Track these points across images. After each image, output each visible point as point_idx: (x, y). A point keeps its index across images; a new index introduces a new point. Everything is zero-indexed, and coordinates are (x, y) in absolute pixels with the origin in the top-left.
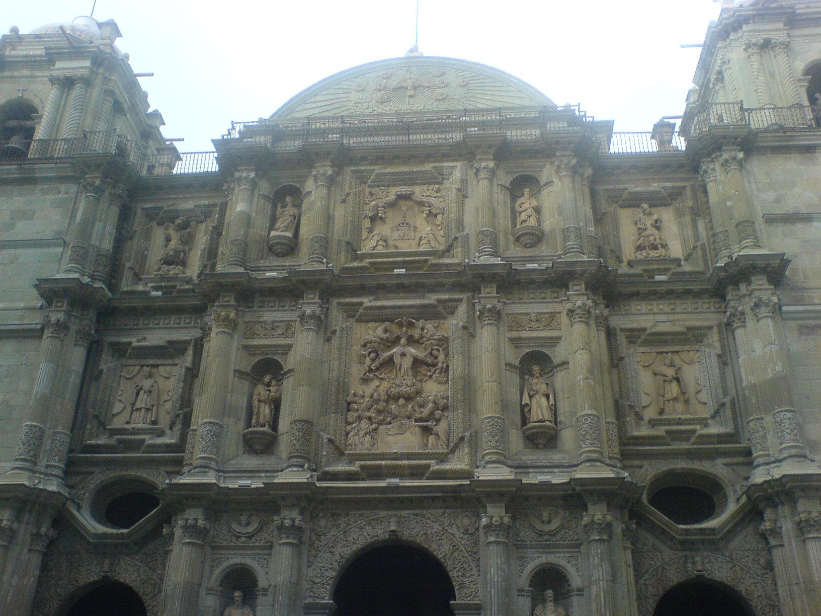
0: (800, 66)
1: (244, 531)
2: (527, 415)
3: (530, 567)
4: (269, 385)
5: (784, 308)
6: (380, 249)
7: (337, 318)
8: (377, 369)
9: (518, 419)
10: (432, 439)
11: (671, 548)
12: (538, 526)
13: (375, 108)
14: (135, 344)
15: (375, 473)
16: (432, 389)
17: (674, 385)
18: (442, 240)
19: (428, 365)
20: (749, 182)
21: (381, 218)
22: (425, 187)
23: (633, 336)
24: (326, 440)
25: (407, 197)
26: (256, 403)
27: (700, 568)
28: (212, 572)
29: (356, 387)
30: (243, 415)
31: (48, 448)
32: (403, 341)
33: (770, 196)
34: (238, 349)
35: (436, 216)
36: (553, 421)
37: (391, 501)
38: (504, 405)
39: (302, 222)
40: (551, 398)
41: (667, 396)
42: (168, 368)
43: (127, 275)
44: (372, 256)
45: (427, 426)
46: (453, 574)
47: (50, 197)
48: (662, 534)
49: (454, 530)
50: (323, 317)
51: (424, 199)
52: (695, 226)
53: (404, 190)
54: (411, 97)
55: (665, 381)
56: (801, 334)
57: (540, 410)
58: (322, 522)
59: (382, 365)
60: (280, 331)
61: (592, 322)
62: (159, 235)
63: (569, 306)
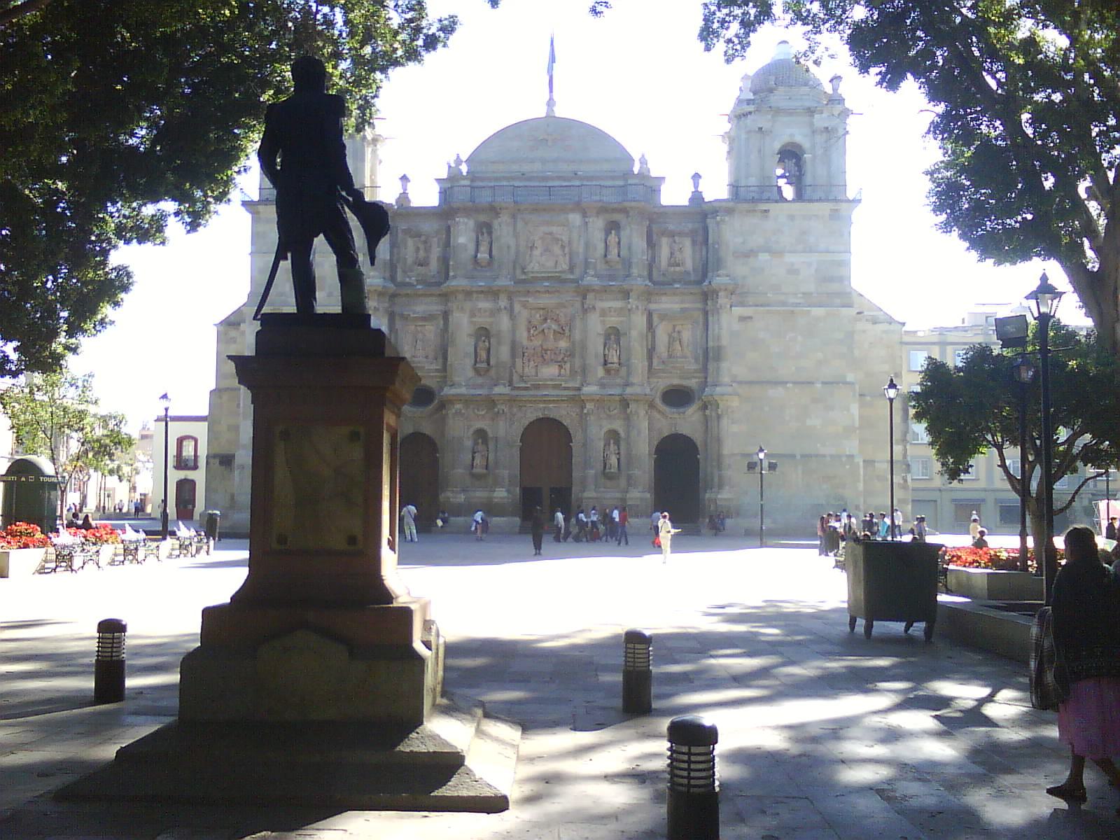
0: (777, 146)
3: (605, 430)
4: (484, 341)
6: (536, 268)
7: (517, 307)
8: (537, 335)
9: (602, 360)
14: (412, 316)
15: (537, 387)
16: (563, 344)
17: (678, 342)
18: (567, 261)
21: (536, 247)
22: (559, 228)
23: (664, 317)
25: (551, 234)
26: (478, 349)
28: (468, 429)
29: (525, 342)
32: (549, 321)
33: (740, 240)
38: (596, 356)
40: (618, 351)
44: (532, 272)
49: (572, 413)
51: (558, 236)
59: (539, 333)
60: (487, 313)
61: (640, 313)
62: (410, 243)
63: (629, 306)
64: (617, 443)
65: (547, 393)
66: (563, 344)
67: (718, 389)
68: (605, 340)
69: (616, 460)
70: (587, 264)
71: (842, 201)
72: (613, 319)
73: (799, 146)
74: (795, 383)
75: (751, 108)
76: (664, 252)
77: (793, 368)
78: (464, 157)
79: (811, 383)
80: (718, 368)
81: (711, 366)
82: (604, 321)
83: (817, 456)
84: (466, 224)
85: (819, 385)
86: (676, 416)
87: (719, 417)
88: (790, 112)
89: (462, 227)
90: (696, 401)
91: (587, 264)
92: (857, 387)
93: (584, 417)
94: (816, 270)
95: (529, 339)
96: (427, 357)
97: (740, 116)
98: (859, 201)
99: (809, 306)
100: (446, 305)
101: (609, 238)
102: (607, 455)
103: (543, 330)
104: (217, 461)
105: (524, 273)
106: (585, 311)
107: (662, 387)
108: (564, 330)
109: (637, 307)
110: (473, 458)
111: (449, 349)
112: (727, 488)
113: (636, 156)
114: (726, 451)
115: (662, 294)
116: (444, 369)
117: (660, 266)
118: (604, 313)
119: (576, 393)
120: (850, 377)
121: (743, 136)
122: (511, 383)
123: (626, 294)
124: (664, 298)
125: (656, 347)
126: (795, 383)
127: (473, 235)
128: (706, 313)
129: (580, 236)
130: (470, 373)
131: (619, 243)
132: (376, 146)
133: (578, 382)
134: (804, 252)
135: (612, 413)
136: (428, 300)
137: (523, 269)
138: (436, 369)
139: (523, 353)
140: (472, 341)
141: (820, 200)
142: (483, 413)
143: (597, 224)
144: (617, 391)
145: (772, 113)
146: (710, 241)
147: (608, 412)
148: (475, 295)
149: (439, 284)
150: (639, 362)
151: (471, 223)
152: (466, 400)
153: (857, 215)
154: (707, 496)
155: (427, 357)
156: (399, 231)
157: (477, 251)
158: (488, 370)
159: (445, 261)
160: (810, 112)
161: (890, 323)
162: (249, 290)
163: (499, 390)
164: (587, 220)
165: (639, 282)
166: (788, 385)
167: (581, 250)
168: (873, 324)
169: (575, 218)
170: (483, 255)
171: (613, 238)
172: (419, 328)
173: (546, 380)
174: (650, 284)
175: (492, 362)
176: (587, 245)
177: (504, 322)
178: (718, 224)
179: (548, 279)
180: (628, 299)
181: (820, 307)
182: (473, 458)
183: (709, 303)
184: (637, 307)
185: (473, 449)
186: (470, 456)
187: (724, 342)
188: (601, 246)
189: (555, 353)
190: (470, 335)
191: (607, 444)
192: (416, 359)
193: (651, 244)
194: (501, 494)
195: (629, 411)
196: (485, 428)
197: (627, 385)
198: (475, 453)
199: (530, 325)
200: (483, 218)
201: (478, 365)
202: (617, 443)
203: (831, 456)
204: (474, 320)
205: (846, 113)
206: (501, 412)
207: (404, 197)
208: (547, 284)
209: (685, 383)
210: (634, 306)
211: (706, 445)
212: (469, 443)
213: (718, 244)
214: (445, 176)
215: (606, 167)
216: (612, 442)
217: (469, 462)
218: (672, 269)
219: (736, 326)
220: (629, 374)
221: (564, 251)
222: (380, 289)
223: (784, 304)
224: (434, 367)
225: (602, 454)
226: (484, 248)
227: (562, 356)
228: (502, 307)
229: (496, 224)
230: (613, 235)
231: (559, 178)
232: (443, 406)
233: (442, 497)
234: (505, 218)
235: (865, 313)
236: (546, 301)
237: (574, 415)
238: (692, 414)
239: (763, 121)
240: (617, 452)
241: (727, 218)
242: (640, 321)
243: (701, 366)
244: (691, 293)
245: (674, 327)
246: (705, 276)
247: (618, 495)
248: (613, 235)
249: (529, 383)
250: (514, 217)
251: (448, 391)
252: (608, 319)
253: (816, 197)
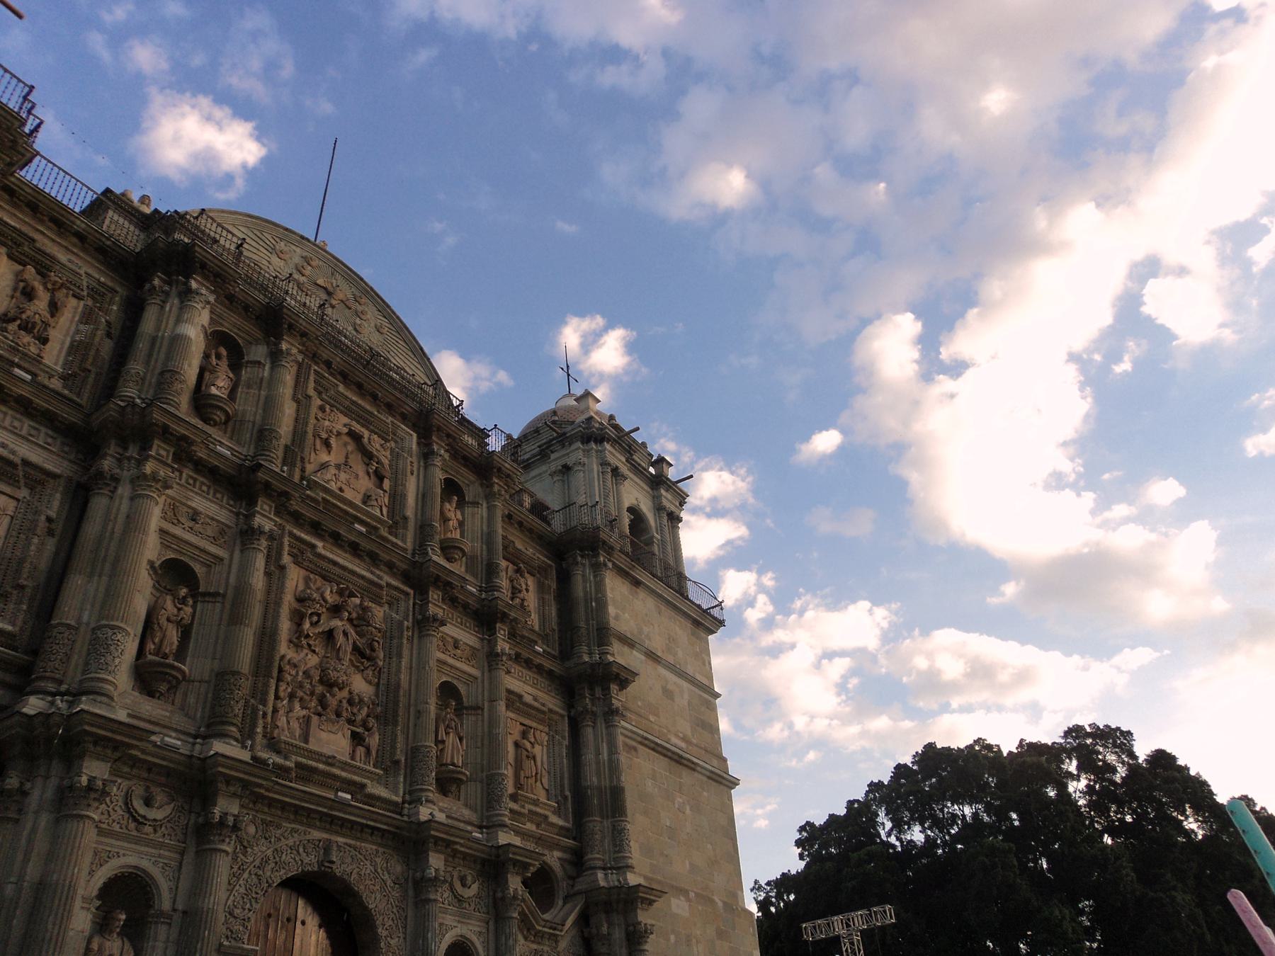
4: (183, 601)
10: (360, 751)
11: (526, 938)
28: (91, 873)
44: (326, 490)
108: (373, 650)
213: (597, 600)
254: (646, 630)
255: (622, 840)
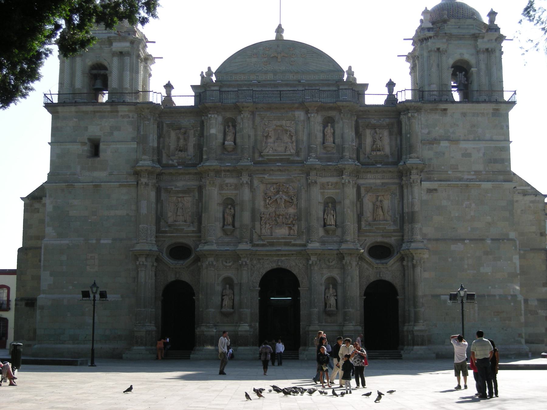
0: (451, 62)
1: (228, 264)
2: (325, 222)
3: (325, 277)
4: (230, 209)
5: (422, 182)
7: (256, 183)
9: (322, 223)
12: (328, 264)
13: (263, 68)
15: (272, 244)
16: (292, 210)
17: (380, 208)
18: (295, 148)
19: (290, 202)
20: (418, 124)
24: (254, 232)
25: (281, 126)
27: (381, 276)
28: (218, 278)
29: (262, 209)
30: (222, 220)
31: (150, 233)
32: (281, 193)
33: (425, 131)
34: (217, 195)
35: (292, 136)
36: (335, 224)
37: (278, 255)
39: (237, 136)
40: (335, 216)
41: (377, 213)
42: (188, 198)
43: (164, 155)
44: (268, 155)
45: (290, 227)
46: (299, 279)
47: (126, 120)
48: (370, 264)
50: (249, 183)
51: (287, 128)
52: (396, 140)
53: (279, 123)
54: (280, 62)
55: (377, 208)
56: (427, 192)
57: (331, 221)
58: (255, 262)
60: (233, 187)
62: (173, 134)
63: (343, 181)
64: (335, 286)
65: (280, 248)
66: (292, 210)
67: (413, 244)
68: (325, 207)
69: (335, 301)
70: (310, 149)
71: (501, 102)
72: (329, 191)
73: (467, 63)
74: (471, 240)
75: (431, 34)
76: (368, 141)
77: (469, 229)
78: (214, 70)
79: (482, 240)
80: (412, 229)
81: (407, 227)
82: (324, 192)
83: (489, 296)
84: (216, 119)
85: (489, 242)
86: (380, 266)
87: (414, 266)
88: (461, 37)
89: (213, 121)
90: (395, 254)
91: (310, 149)
92: (518, 242)
93: (309, 267)
94: (484, 155)
95: (266, 206)
96: (185, 221)
97: (422, 39)
98: (514, 103)
99: (480, 181)
100: (201, 181)
101: (326, 130)
102: (327, 297)
103: (276, 200)
104: (23, 303)
105: (261, 156)
106: (309, 185)
107: (368, 244)
108: (292, 200)
109: (349, 182)
110: (222, 300)
111: (203, 215)
112: (422, 321)
113: (345, 69)
114: (420, 293)
115: (368, 172)
116: (199, 230)
117: (366, 151)
118: (323, 186)
119: (303, 248)
120: (512, 235)
121: (425, 54)
122: (251, 241)
123: (340, 172)
124: (369, 176)
125: (364, 213)
126: (471, 240)
127: (222, 128)
128: (401, 187)
129: (304, 128)
130: (219, 233)
131: (334, 133)
132: (146, 63)
133: (304, 240)
134: (474, 140)
135: (331, 264)
136: (187, 177)
137: (260, 153)
138: (193, 231)
139: (261, 218)
140: (221, 209)
141: (485, 102)
142: (230, 264)
143: (317, 119)
144: (335, 247)
145: (447, 37)
146: (404, 132)
147: (328, 264)
148: (223, 173)
149: (195, 165)
150: (351, 225)
151: (220, 119)
152: (217, 255)
153: (513, 115)
154: (405, 328)
155: (185, 221)
156: (165, 125)
157: (224, 140)
158: (233, 231)
159: (199, 148)
160: (475, 37)
161: (536, 196)
162: (48, 171)
163: (243, 246)
164: (309, 115)
165: (350, 163)
166: (466, 241)
167: (305, 138)
168: (523, 195)
169: (300, 115)
170: (229, 143)
171: (329, 130)
172: (179, 199)
173: (278, 239)
174: (359, 164)
175: (237, 224)
176: (309, 135)
177: (246, 194)
178: (409, 119)
179: (281, 160)
180: (342, 175)
181: (487, 181)
182: (222, 300)
183: (404, 178)
184: (349, 182)
185: (222, 293)
186: (220, 298)
187: (417, 208)
188: (320, 136)
189: (286, 218)
190: (219, 204)
191: (327, 288)
192: (177, 223)
193: (359, 134)
194: (244, 328)
195: (344, 262)
196: (233, 277)
197: (342, 242)
198: (224, 296)
199: (266, 196)
200: (228, 115)
201: (225, 227)
202: (335, 286)
203: (500, 295)
204: (224, 192)
205: (502, 38)
206: (244, 263)
207: (168, 99)
208: (280, 164)
209: (386, 240)
210: (347, 181)
211: (404, 288)
212: (219, 288)
213: (410, 133)
214: (199, 83)
215: (322, 77)
216: (331, 286)
217: (219, 303)
218: (375, 153)
219: (425, 197)
220: (344, 233)
221: (291, 139)
222: (150, 168)
223: (460, 180)
224: (191, 229)
225: (323, 296)
226: (230, 137)
227: (291, 219)
228: (245, 182)
229: (239, 119)
230: (329, 127)
231: (287, 85)
232: (198, 259)
233: (198, 331)
234: (246, 114)
235: (518, 188)
236: (281, 178)
237: (301, 266)
238: (392, 263)
239: (441, 44)
240: (335, 294)
241: (416, 115)
242: (351, 192)
243: (398, 227)
244: (390, 171)
245: (378, 196)
246: (400, 158)
247: (337, 328)
248: (329, 127)
249: (266, 241)
250: (253, 113)
251: (201, 247)
252: (326, 191)
253: (481, 98)
254: (451, 130)
255: (413, 232)
